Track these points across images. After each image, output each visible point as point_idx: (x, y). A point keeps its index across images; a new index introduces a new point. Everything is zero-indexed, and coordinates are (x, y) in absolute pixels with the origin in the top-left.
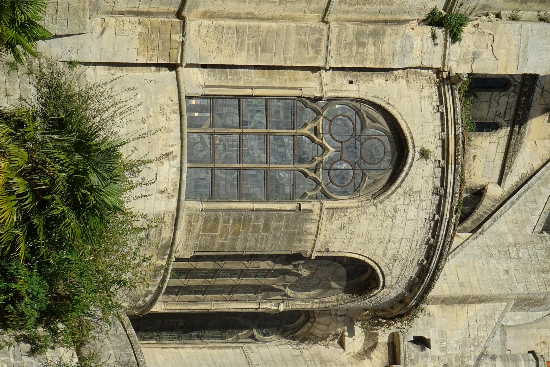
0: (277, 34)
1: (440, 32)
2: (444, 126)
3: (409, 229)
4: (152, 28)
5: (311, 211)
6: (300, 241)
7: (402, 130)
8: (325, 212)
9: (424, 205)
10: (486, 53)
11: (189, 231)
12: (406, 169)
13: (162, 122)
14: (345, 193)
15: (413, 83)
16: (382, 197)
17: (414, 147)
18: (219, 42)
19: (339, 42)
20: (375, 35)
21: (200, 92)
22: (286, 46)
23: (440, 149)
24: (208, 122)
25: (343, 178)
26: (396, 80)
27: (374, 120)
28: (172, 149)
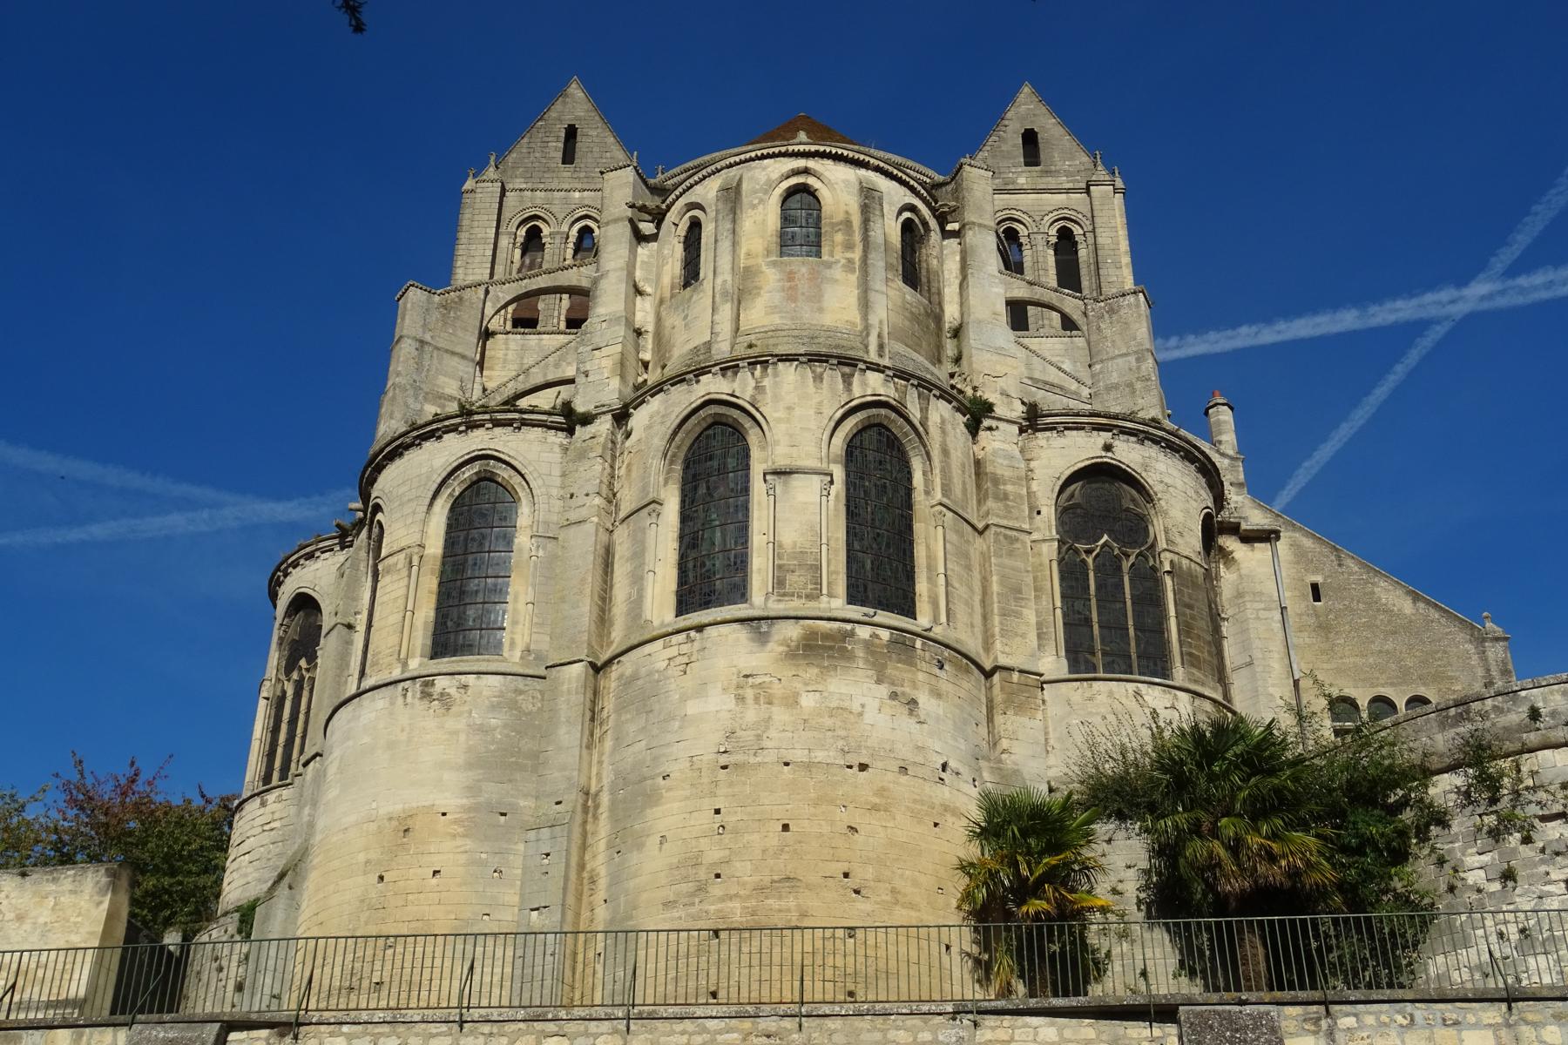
0: (1004, 578)
1: (986, 423)
2: (1078, 427)
3: (1176, 473)
4: (1009, 702)
5: (1171, 562)
6: (1196, 577)
7: (1085, 467)
8: (1171, 548)
9: (1154, 455)
10: (1001, 383)
11: (1203, 685)
12: (1124, 467)
13: (1102, 698)
14: (1146, 530)
15: (1033, 455)
16: (1151, 492)
17: (1101, 457)
18: (1016, 635)
19: (1005, 517)
20: (996, 481)
21: (1065, 662)
22: (1013, 569)
23: (1101, 433)
24: (1089, 656)
25: (1131, 530)
26: (1031, 471)
27: (1072, 496)
28: (1130, 691)
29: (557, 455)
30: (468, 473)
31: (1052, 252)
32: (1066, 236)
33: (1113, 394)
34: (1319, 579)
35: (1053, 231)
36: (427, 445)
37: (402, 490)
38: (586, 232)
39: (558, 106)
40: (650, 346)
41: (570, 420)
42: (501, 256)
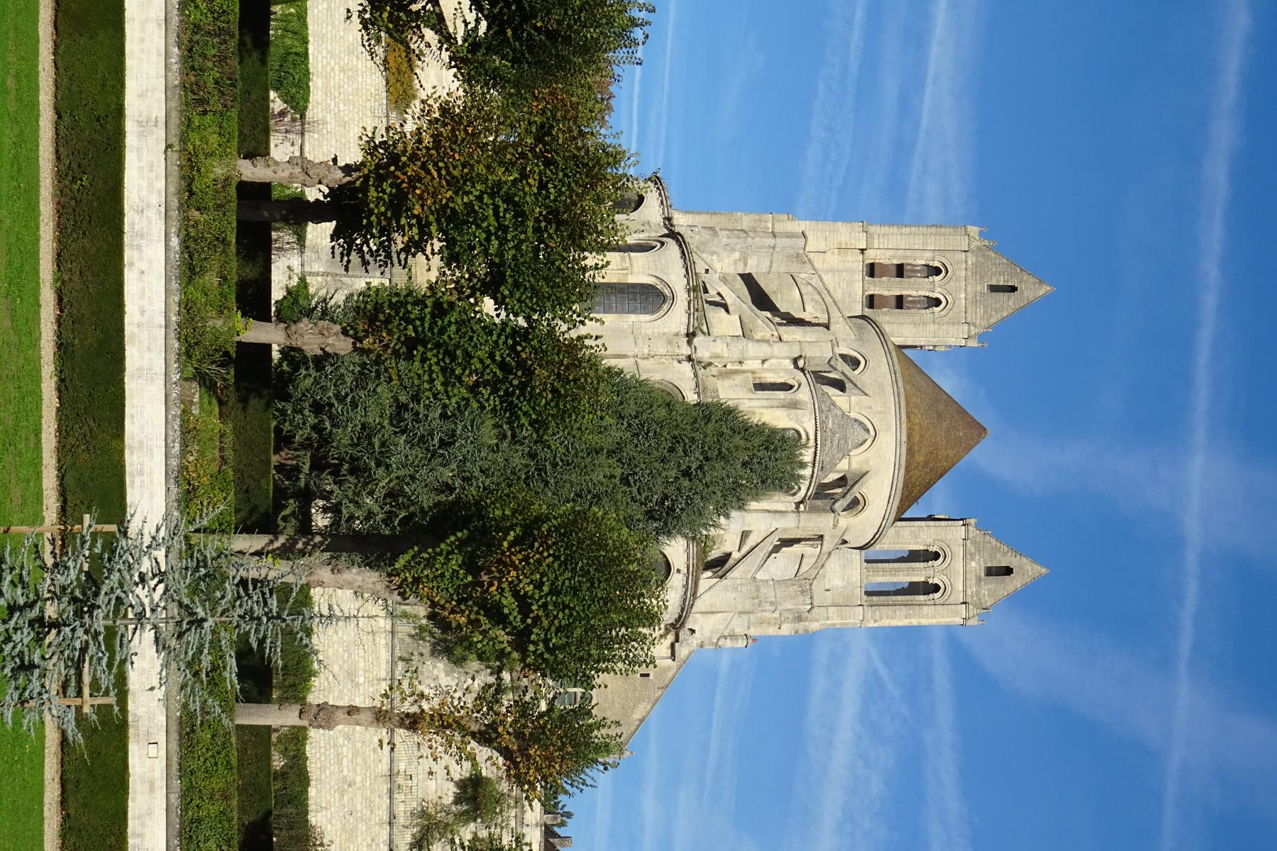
29: (674, 330)
30: (667, 292)
31: (922, 579)
32: (936, 588)
33: (754, 589)
34: (651, 677)
35: (936, 581)
36: (684, 271)
37: (663, 261)
38: (937, 302)
39: (1032, 280)
40: (734, 368)
41: (690, 336)
42: (918, 254)
